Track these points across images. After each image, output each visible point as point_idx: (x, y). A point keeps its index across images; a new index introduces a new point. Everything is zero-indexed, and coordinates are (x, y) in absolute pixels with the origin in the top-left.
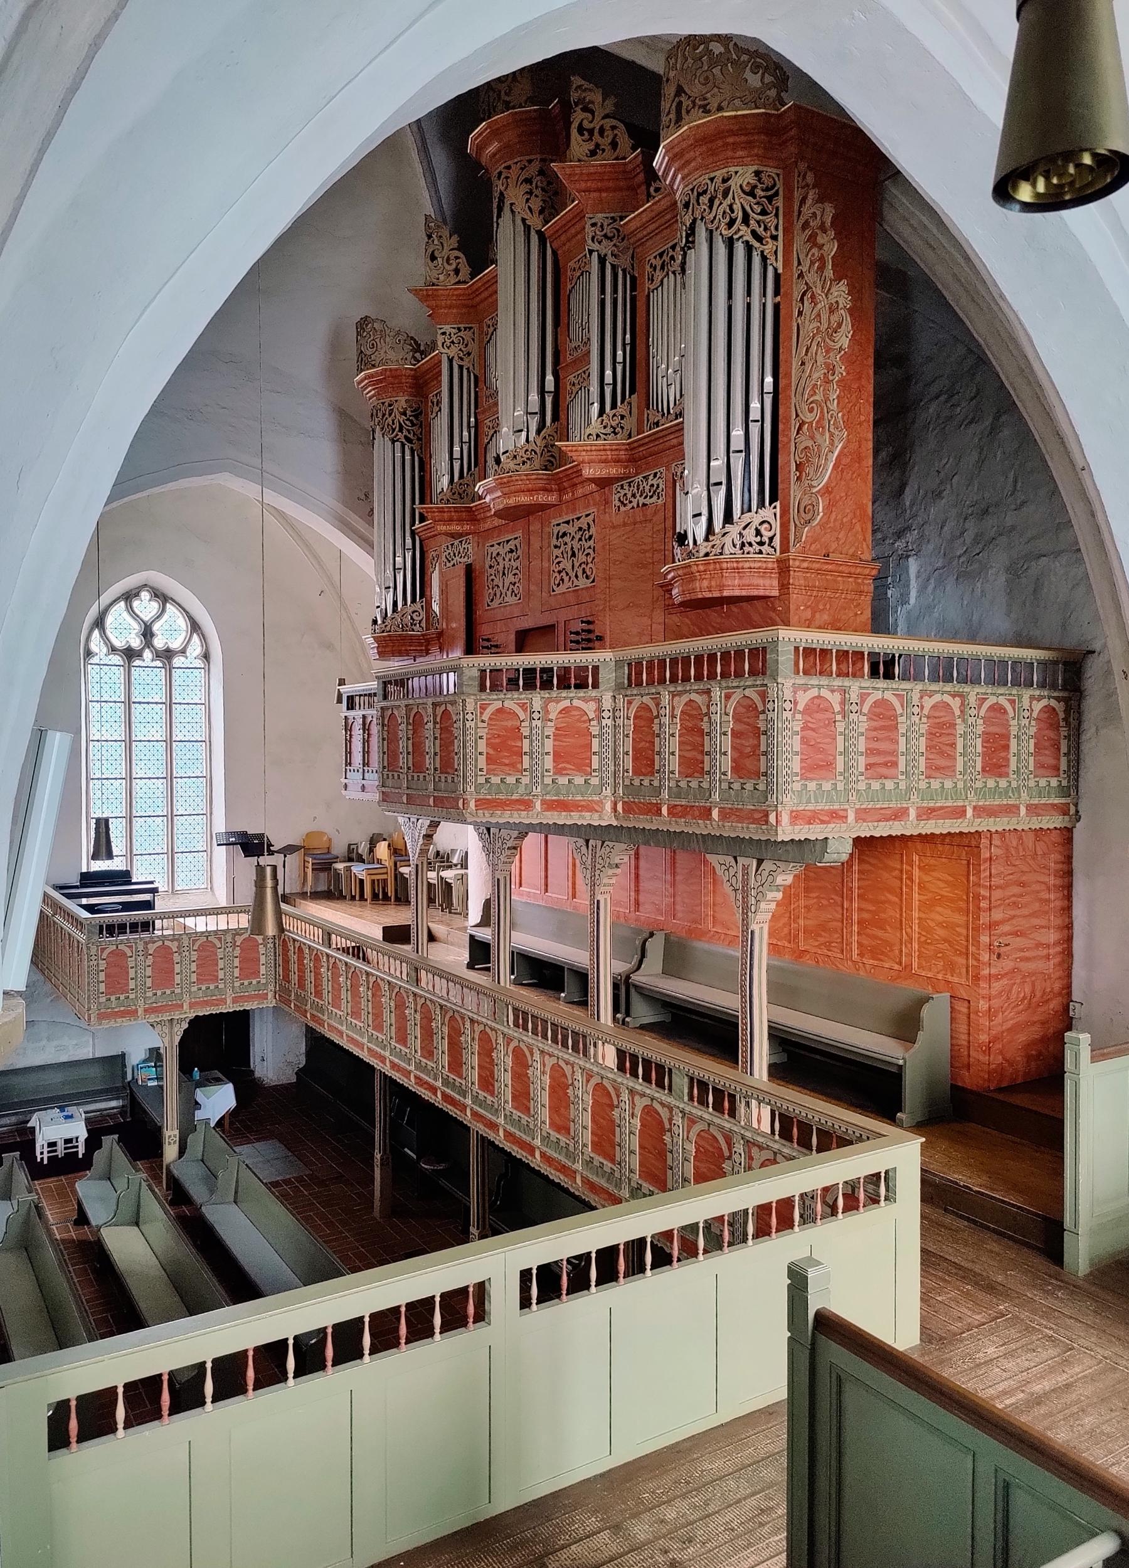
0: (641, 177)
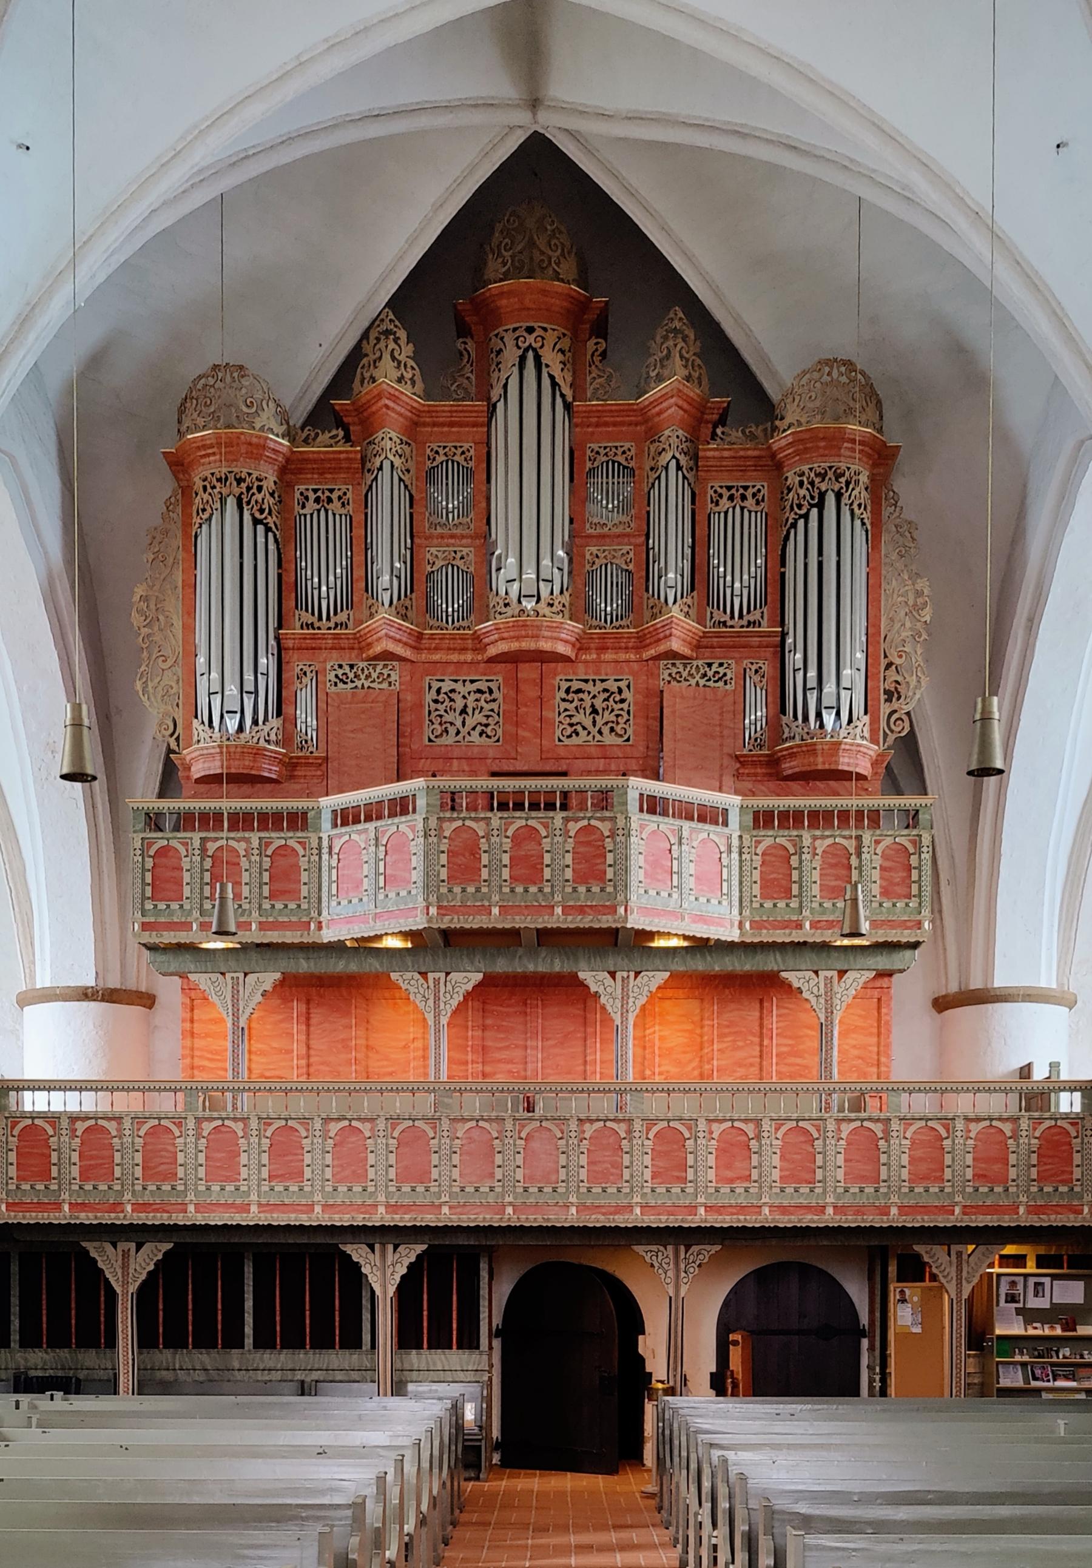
0: (716, 417)
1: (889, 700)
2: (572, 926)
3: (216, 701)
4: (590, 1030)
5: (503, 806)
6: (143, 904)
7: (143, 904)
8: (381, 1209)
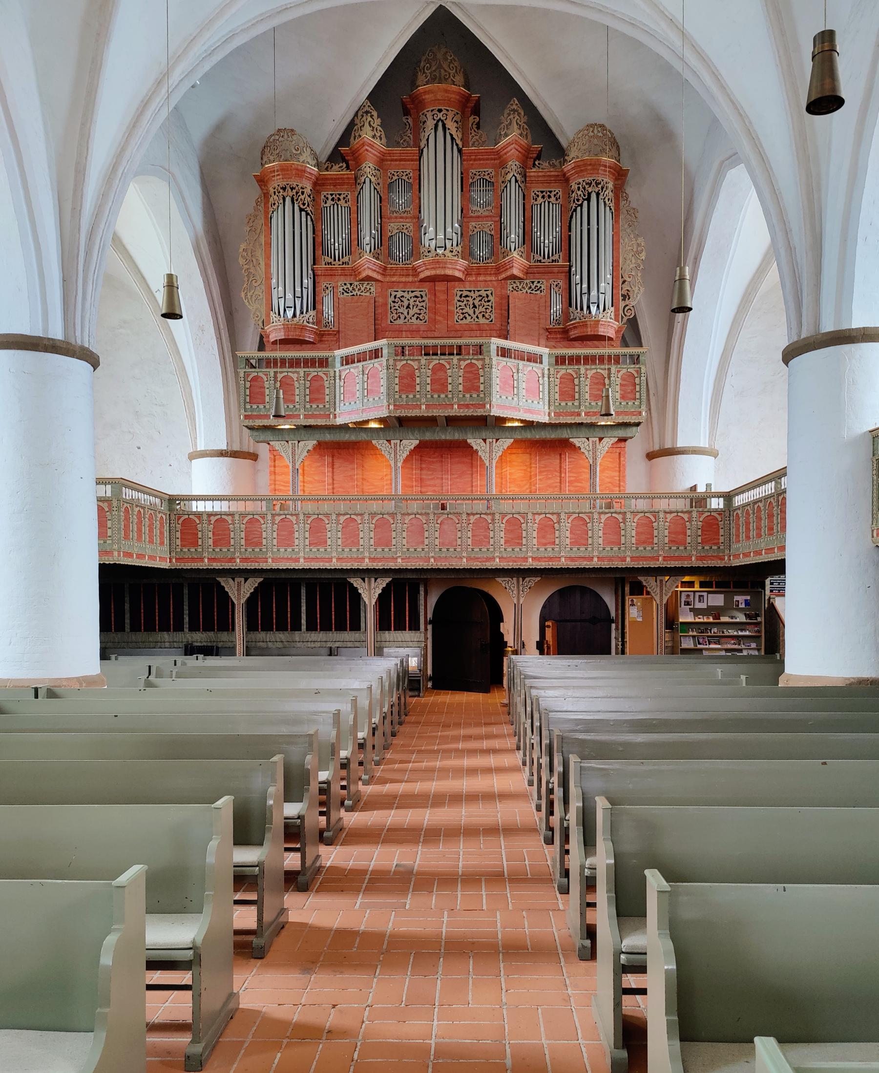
1: (624, 300)
3: (282, 301)
4: (474, 470)
8: (367, 560)
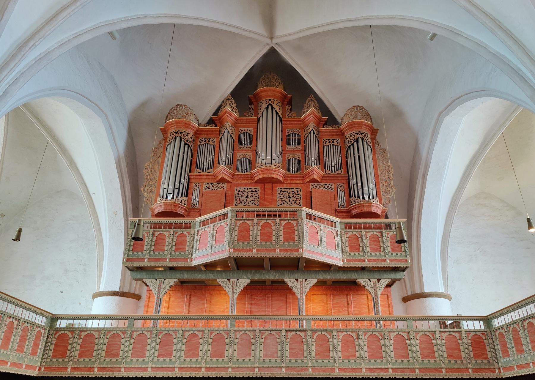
2: (283, 256)
4: (288, 305)
5: (258, 216)
6: (128, 252)
7: (128, 252)
